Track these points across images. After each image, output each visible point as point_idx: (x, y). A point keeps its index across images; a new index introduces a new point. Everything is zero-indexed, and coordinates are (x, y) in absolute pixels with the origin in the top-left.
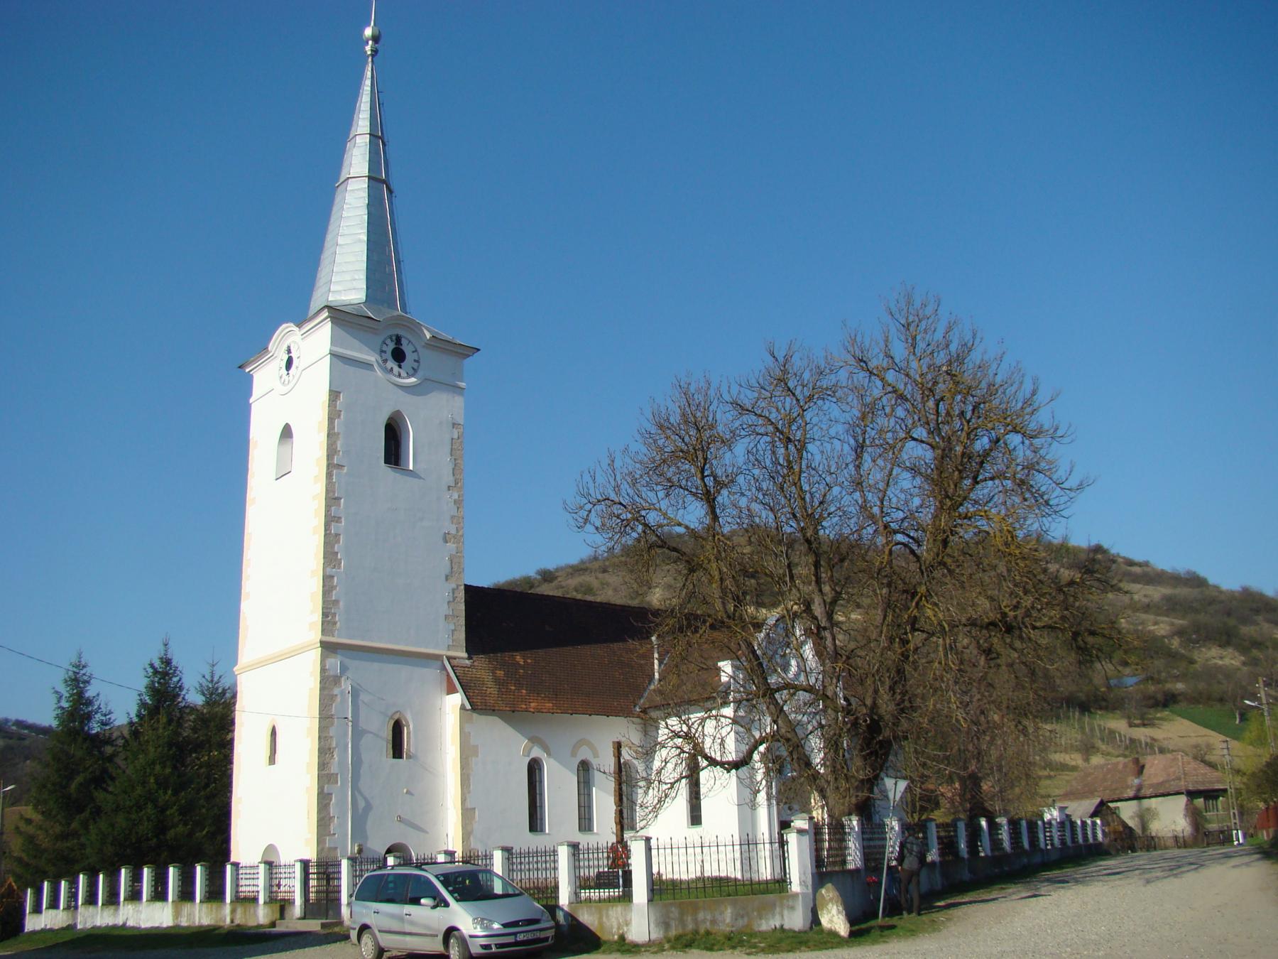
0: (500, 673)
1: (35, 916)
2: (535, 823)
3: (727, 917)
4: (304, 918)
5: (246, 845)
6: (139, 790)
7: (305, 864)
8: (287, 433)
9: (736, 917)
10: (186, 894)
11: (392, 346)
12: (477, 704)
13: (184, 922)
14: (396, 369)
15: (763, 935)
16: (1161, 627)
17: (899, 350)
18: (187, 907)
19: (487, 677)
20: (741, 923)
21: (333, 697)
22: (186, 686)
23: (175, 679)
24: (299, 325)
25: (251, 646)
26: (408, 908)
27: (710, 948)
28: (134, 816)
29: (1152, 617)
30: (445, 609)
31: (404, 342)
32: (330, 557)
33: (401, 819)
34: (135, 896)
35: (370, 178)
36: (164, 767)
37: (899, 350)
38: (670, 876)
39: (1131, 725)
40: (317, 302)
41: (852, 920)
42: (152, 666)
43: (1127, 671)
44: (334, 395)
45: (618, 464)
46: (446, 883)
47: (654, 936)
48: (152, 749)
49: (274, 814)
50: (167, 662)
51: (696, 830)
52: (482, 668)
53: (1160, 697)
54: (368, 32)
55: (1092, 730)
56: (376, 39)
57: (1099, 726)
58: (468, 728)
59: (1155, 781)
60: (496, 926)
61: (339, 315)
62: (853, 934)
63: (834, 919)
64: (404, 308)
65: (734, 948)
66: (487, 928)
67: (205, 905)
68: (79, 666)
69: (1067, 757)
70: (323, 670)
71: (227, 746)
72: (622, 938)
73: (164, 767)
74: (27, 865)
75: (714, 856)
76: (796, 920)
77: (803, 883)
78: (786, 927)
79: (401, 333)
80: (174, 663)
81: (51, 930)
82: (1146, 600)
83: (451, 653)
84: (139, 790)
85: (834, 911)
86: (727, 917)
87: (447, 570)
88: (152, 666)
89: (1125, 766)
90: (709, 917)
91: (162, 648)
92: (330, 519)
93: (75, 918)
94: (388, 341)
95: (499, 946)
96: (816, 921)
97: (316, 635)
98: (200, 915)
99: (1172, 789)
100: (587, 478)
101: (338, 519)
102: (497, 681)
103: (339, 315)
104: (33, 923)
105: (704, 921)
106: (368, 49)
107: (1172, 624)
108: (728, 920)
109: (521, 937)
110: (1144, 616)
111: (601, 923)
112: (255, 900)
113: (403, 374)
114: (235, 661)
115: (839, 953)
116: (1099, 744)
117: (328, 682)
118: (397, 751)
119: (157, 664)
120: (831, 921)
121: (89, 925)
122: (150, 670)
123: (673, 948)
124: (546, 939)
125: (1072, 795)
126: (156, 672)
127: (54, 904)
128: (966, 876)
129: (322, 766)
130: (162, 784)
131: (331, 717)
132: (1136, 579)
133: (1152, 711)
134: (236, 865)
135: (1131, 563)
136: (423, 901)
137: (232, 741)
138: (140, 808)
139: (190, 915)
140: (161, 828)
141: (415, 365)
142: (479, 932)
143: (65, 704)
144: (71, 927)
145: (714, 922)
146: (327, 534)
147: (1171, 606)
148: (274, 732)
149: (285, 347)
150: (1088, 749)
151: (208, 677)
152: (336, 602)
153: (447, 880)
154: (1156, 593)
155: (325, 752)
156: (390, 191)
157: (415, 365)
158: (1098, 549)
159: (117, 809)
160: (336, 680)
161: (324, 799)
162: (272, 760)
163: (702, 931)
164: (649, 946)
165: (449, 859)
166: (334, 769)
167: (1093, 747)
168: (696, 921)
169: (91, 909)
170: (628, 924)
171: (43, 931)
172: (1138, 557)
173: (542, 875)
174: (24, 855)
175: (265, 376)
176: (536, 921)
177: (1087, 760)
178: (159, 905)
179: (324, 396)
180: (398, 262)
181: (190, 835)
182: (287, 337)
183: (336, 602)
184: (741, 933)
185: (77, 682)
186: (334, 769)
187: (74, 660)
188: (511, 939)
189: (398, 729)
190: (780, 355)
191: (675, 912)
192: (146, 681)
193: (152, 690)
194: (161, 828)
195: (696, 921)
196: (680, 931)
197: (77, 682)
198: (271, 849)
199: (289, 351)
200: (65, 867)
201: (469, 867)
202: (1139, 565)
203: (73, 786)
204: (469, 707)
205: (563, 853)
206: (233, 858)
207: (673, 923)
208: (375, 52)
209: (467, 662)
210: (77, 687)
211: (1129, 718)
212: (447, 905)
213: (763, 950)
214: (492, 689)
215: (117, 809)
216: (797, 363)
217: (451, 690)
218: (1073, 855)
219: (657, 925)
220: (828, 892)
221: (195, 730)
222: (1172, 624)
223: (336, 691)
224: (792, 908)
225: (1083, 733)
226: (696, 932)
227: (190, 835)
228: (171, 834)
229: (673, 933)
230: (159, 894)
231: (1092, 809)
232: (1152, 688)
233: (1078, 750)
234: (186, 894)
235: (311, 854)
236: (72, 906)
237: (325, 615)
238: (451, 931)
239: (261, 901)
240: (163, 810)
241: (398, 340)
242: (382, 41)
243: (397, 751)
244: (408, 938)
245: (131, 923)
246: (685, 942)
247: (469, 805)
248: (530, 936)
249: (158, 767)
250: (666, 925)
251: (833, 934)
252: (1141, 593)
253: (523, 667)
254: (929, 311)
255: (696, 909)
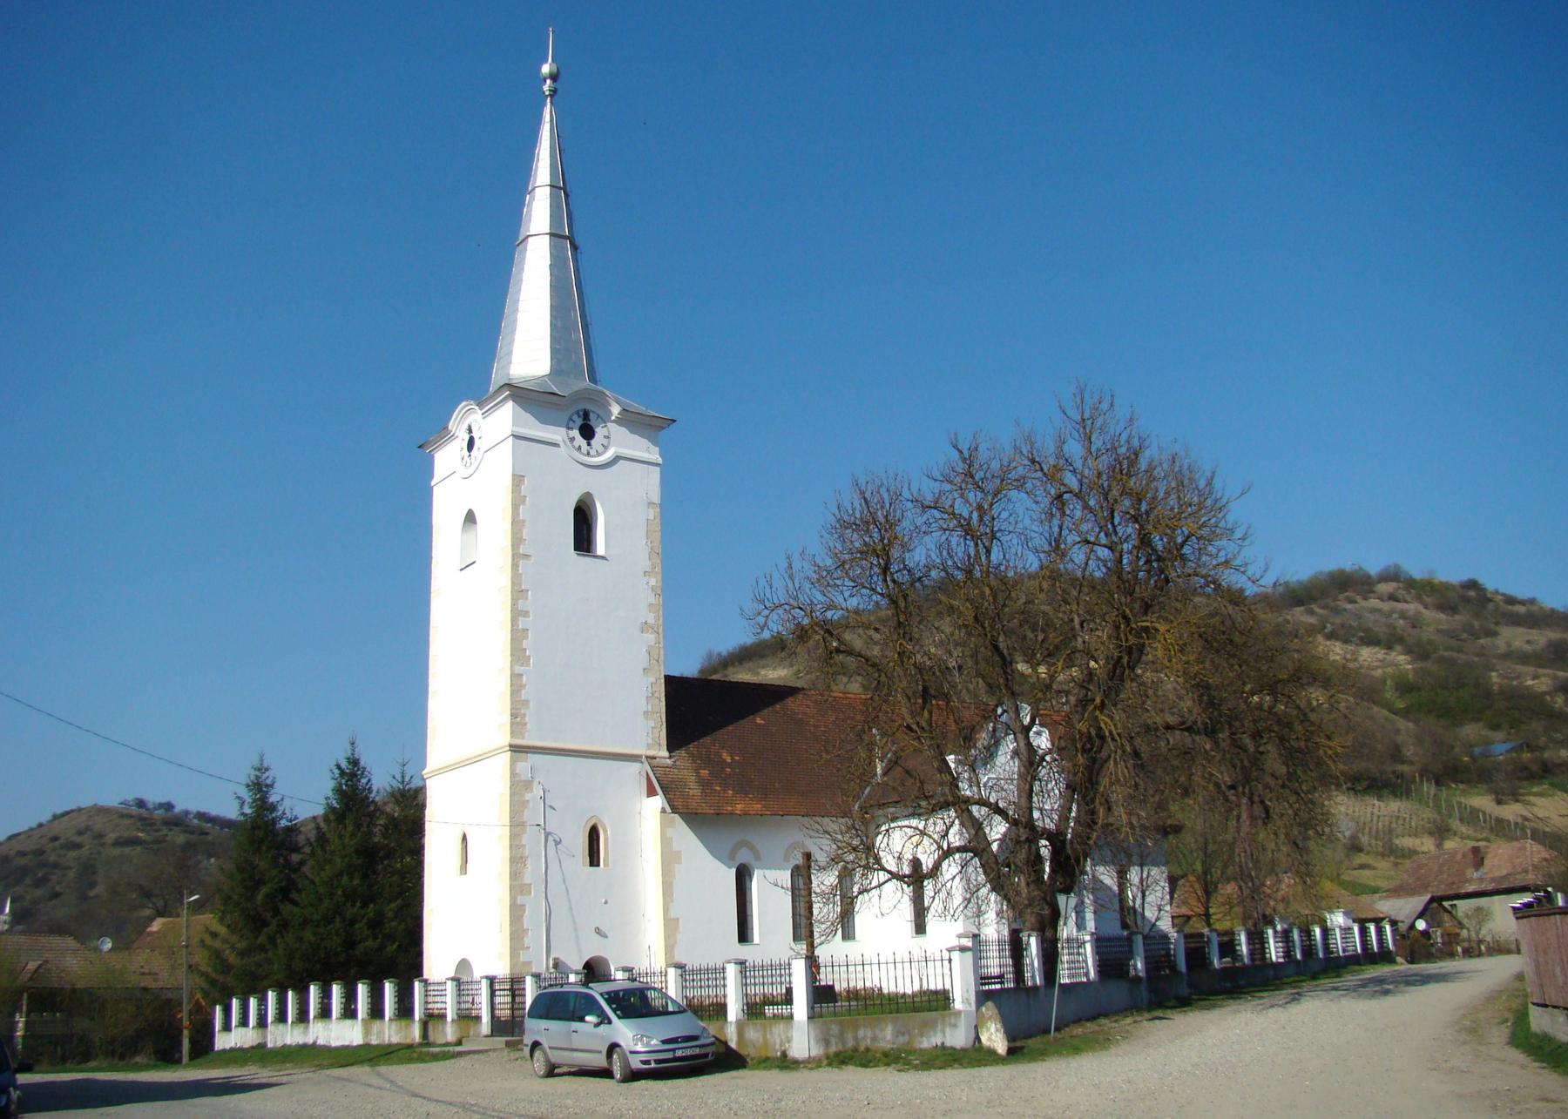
0: (705, 773)
1: (225, 1034)
2: (744, 935)
3: (886, 1035)
4: (492, 1035)
5: (438, 961)
6: (327, 903)
7: (492, 980)
8: (470, 518)
9: (898, 1033)
10: (376, 1012)
11: (579, 422)
12: (681, 806)
13: (374, 1042)
14: (585, 447)
15: (922, 1052)
16: (1539, 682)
17: (1074, 449)
18: (376, 1025)
19: (691, 778)
20: (902, 1040)
21: (525, 803)
22: (375, 788)
23: (364, 781)
24: (480, 405)
25: (441, 747)
26: (576, 1025)
27: (865, 1064)
28: (322, 930)
29: (1530, 669)
30: (643, 705)
31: (592, 416)
32: (518, 654)
33: (598, 931)
34: (325, 1013)
35: (552, 235)
36: (351, 879)
37: (1074, 449)
38: (893, 989)
39: (1499, 802)
40: (496, 380)
41: (1011, 1036)
42: (338, 767)
43: (1500, 735)
44: (518, 480)
45: (796, 566)
46: (609, 1001)
47: (814, 1053)
48: (339, 860)
49: (466, 926)
50: (354, 762)
51: (920, 939)
52: (683, 766)
53: (1535, 768)
54: (546, 69)
55: (1450, 807)
56: (554, 77)
57: (1459, 803)
58: (670, 832)
59: (1497, 874)
60: (654, 1042)
61: (525, 396)
62: (1011, 1051)
63: (995, 1038)
64: (593, 379)
65: (888, 1065)
66: (648, 1044)
67: (394, 1025)
68: (262, 769)
69: (1418, 842)
70: (513, 774)
71: (418, 852)
72: (784, 1054)
73: (351, 879)
74: (214, 983)
75: (908, 972)
76: (958, 1037)
77: (965, 1001)
78: (948, 1044)
79: (588, 407)
80: (362, 763)
81: (241, 1049)
82: (1527, 648)
83: (651, 753)
84: (327, 903)
85: (993, 1029)
86: (886, 1035)
87: (646, 664)
88: (338, 767)
89: (1464, 856)
90: (869, 1034)
91: (349, 747)
92: (517, 614)
93: (265, 1037)
94: (575, 417)
95: (658, 1061)
96: (978, 1038)
97: (505, 739)
98: (389, 1032)
99: (1517, 884)
100: (762, 582)
101: (526, 614)
102: (701, 782)
103: (522, 395)
104: (223, 1041)
105: (864, 1038)
106: (546, 88)
107: (1555, 678)
108: (889, 1037)
109: (679, 1053)
110: (1520, 668)
111: (765, 1039)
112: (443, 1017)
113: (593, 452)
114: (424, 766)
115: (985, 1071)
116: (1455, 824)
117: (519, 787)
118: (594, 860)
119: (344, 764)
120: (990, 1039)
121: (279, 1044)
122: (337, 772)
123: (830, 1065)
124: (706, 1055)
125: (1398, 891)
126: (343, 773)
127: (244, 1022)
128: (1184, 990)
129: (515, 875)
130: (351, 896)
131: (523, 824)
132: (1516, 620)
133: (1525, 783)
134: (426, 981)
135: (1511, 601)
136: (588, 1018)
137: (422, 847)
138: (328, 921)
139: (380, 1032)
140: (350, 944)
141: (605, 442)
142: (639, 1048)
143: (248, 810)
144: (262, 1046)
145: (874, 1039)
146: (514, 630)
147: (1560, 654)
148: (464, 838)
149: (466, 426)
150: (1440, 832)
151: (399, 777)
152: (525, 703)
153: (614, 999)
154: (1541, 638)
155: (517, 860)
156: (574, 247)
157: (605, 442)
158: (1473, 584)
159: (305, 922)
160: (528, 785)
161: (516, 912)
162: (464, 869)
163: (862, 1048)
164: (812, 1063)
165: (626, 975)
166: (527, 879)
167: (1448, 830)
168: (856, 1038)
169: (281, 1026)
170: (789, 1040)
171: (232, 1050)
172: (1521, 594)
173: (712, 992)
174: (210, 970)
175: (447, 458)
176: (695, 1038)
177: (1439, 846)
178: (348, 1022)
179: (508, 481)
180: (585, 326)
181: (381, 948)
182: (467, 418)
183: (525, 703)
184: (899, 1050)
185: (260, 788)
186: (527, 879)
187: (256, 763)
188: (669, 1055)
189: (594, 835)
190: (965, 447)
191: (835, 1029)
192: (332, 784)
193: (338, 790)
194: (350, 944)
195: (856, 1038)
196: (840, 1047)
197: (260, 788)
198: (464, 965)
199: (470, 430)
200: (253, 985)
201: (636, 985)
202: (1522, 603)
203: (260, 897)
204: (668, 810)
205: (732, 971)
206: (427, 974)
207: (833, 1040)
208: (554, 92)
209: (669, 761)
210: (260, 790)
211: (1497, 793)
212: (610, 1022)
213: (916, 1068)
214: (694, 790)
215: (305, 922)
216: (983, 455)
217: (651, 792)
218: (1315, 967)
219: (817, 1042)
220: (989, 1009)
221: (385, 835)
222: (1555, 678)
223: (528, 796)
224: (955, 1026)
225: (1440, 813)
226: (855, 1050)
227: (381, 948)
228: (360, 949)
229: (833, 1049)
230: (349, 1012)
231: (1420, 908)
232: (1526, 756)
233: (1431, 834)
234: (376, 1012)
235: (502, 969)
236: (262, 1023)
237: (514, 716)
238: (613, 1047)
239: (449, 1019)
240: (353, 922)
241: (586, 415)
242: (561, 79)
243: (594, 860)
244: (576, 1054)
245: (321, 1042)
246: (840, 1059)
247: (673, 915)
248: (689, 1052)
249: (345, 878)
250: (827, 1043)
251: (992, 1052)
252: (1515, 638)
253: (729, 765)
254: (1105, 406)
255: (856, 1028)
